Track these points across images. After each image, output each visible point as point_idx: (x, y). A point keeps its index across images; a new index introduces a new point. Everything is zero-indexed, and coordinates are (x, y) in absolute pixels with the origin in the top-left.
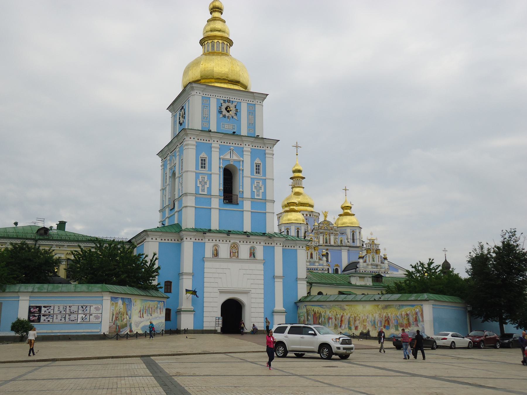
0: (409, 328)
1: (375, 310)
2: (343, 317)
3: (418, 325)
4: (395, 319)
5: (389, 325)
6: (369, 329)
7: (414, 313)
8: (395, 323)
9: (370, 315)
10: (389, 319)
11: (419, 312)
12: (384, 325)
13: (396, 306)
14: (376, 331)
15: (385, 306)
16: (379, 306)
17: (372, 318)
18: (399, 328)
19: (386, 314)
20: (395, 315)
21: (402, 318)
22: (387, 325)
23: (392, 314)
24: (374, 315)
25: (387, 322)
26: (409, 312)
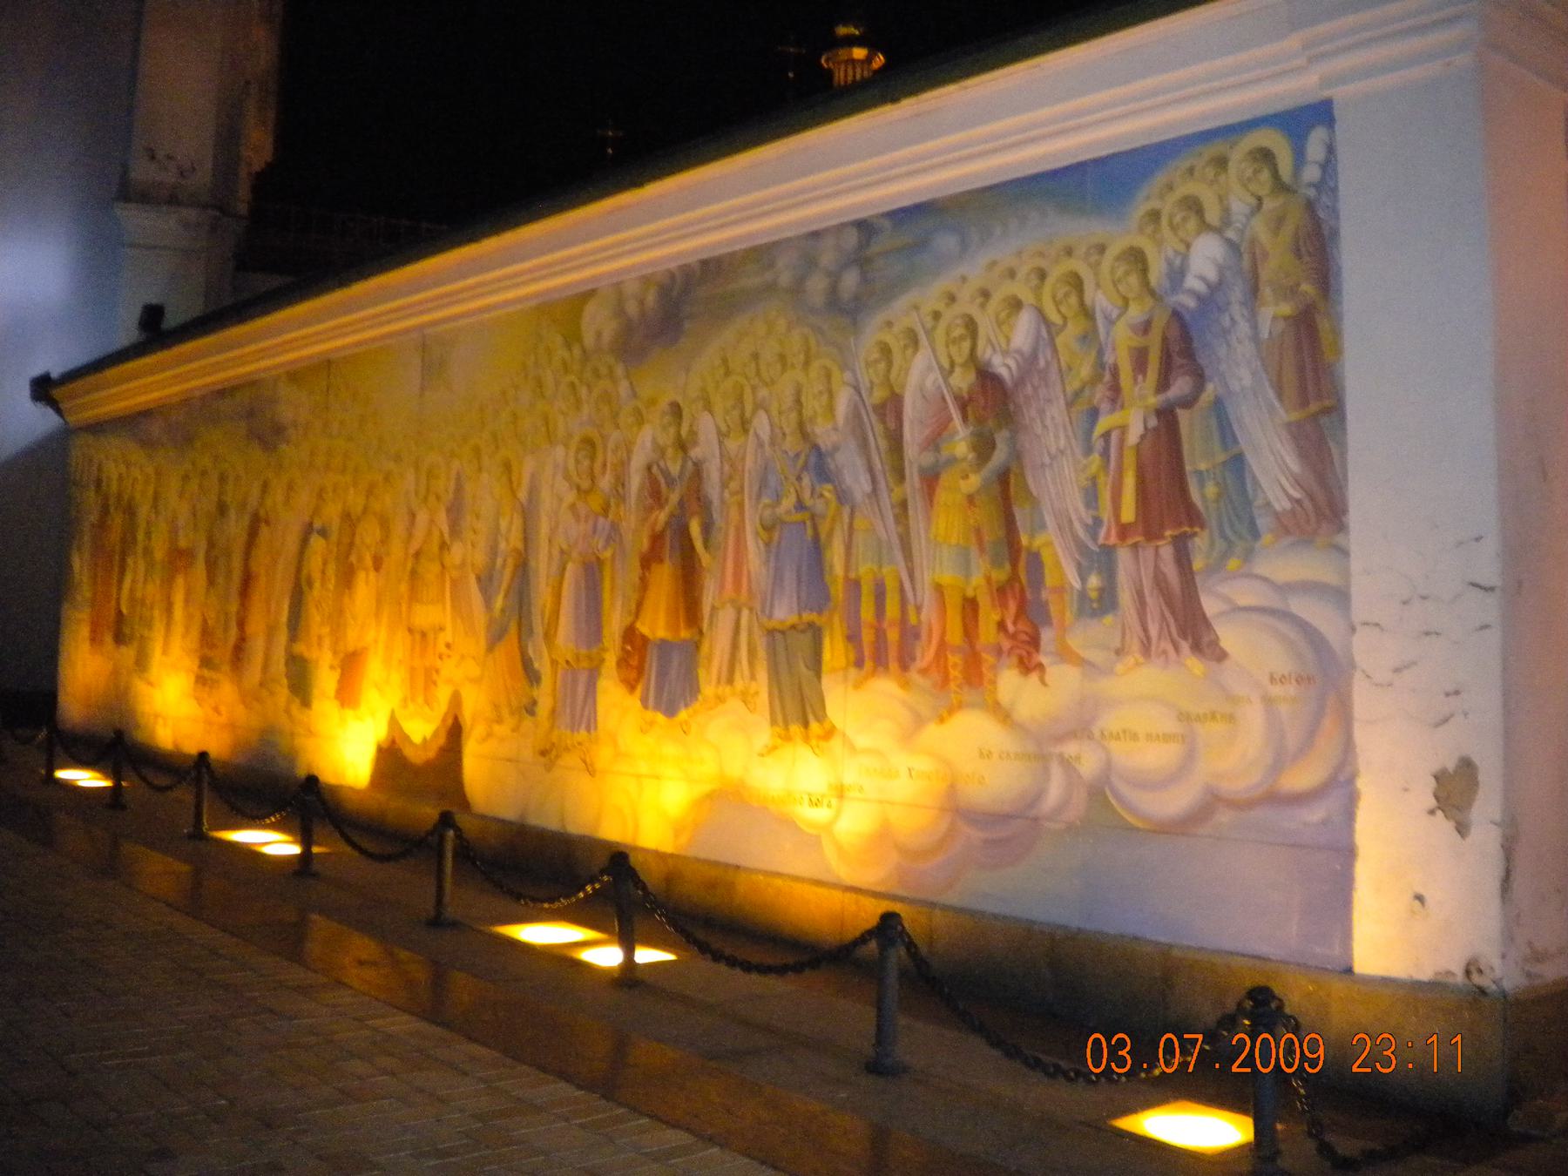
0: (1009, 683)
1: (540, 384)
2: (264, 531)
3: (1210, 606)
4: (788, 502)
5: (685, 634)
6: (456, 700)
7: (1121, 340)
8: (778, 579)
9: (485, 475)
10: (695, 528)
11: (1237, 293)
12: (630, 634)
13: (810, 263)
14: (528, 722)
15: (665, 291)
16: (590, 308)
17: (504, 524)
18: (827, 682)
19: (667, 439)
20: (791, 443)
21: (900, 476)
22: (661, 632)
23: (745, 425)
24: (528, 466)
25: (664, 576)
26: (1023, 331)
